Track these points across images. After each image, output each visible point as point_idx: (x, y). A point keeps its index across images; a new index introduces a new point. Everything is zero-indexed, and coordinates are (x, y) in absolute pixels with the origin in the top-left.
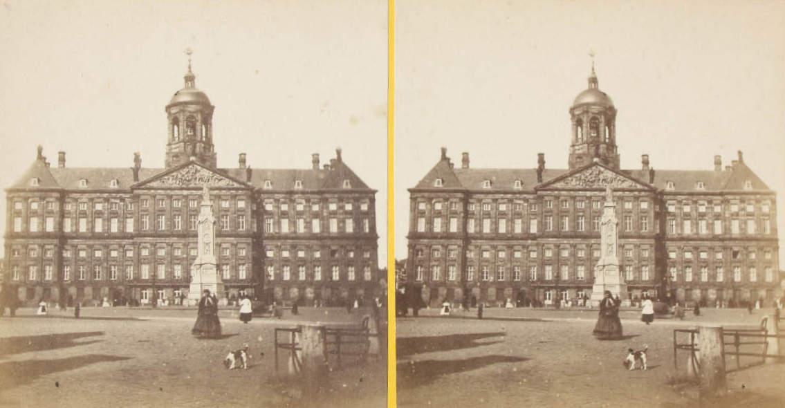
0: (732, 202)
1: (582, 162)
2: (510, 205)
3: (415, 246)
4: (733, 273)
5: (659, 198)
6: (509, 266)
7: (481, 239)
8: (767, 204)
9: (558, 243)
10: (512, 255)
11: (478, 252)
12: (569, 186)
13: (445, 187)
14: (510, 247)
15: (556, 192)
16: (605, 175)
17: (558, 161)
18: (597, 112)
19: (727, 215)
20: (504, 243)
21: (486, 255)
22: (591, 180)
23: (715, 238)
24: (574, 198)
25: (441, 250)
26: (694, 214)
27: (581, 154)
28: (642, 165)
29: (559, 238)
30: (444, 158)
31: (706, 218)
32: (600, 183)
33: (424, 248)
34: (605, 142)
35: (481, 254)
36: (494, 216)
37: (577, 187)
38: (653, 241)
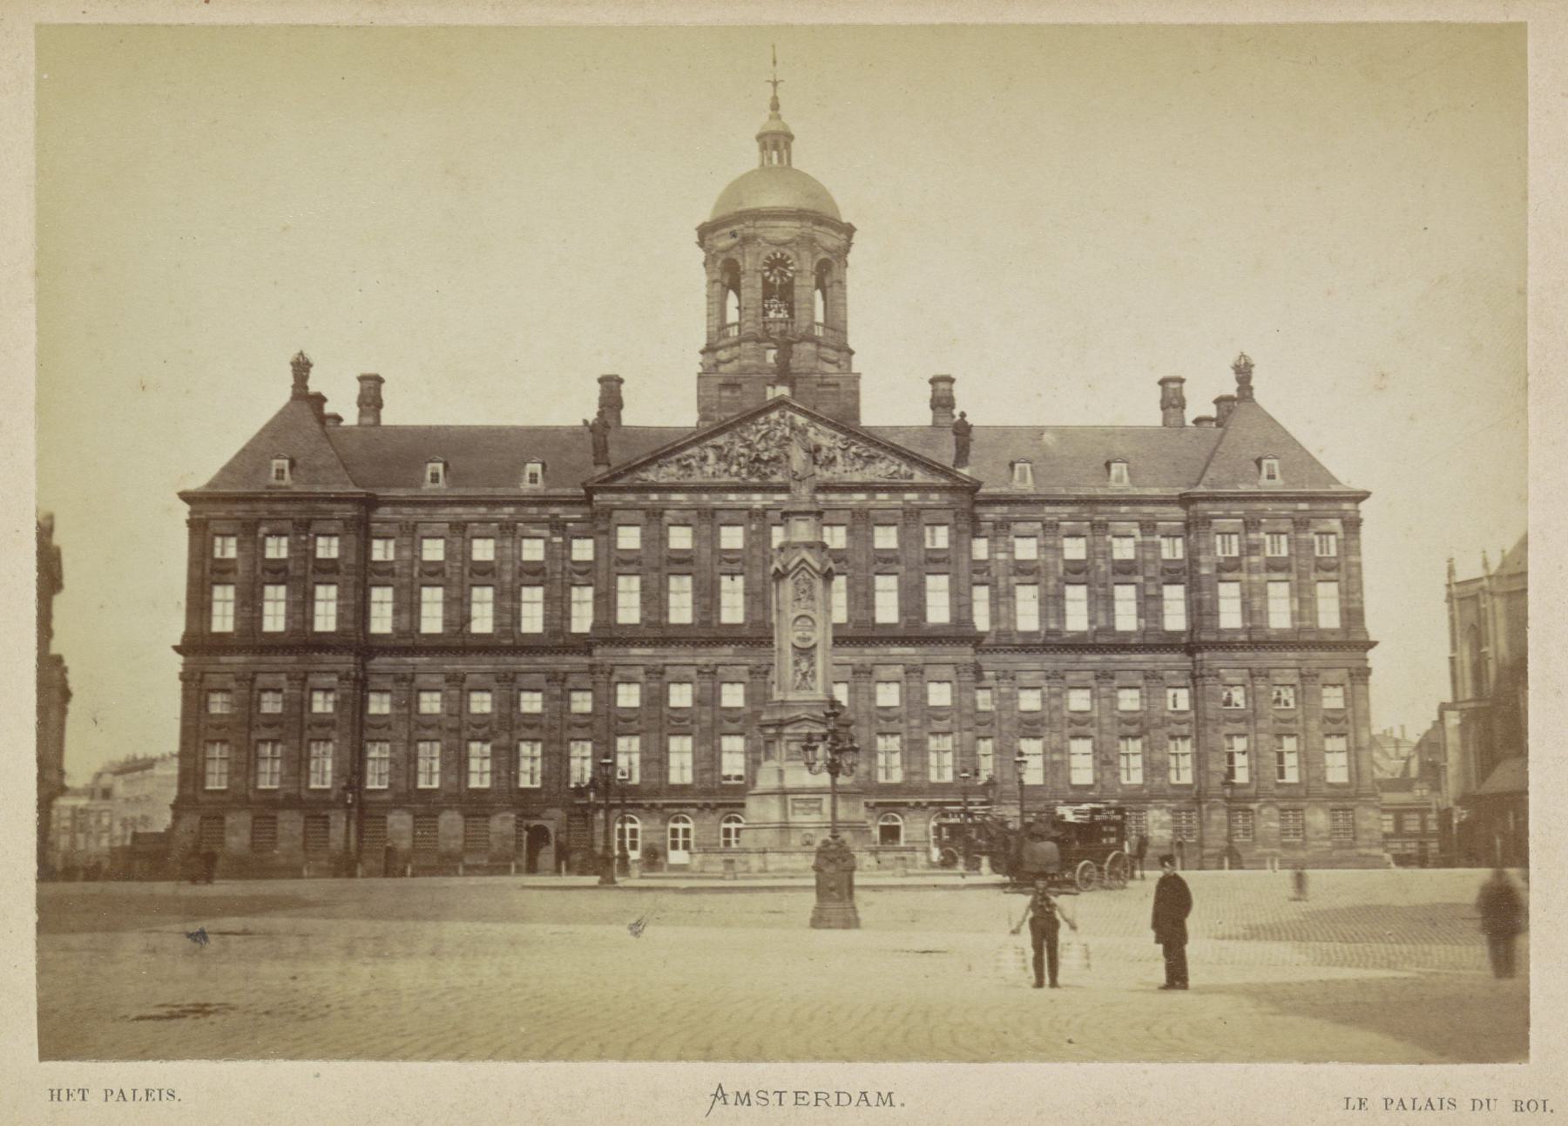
12: (697, 478)
15: (654, 497)
22: (765, 457)
31: (1139, 579)
36: (456, 579)
37: (725, 479)
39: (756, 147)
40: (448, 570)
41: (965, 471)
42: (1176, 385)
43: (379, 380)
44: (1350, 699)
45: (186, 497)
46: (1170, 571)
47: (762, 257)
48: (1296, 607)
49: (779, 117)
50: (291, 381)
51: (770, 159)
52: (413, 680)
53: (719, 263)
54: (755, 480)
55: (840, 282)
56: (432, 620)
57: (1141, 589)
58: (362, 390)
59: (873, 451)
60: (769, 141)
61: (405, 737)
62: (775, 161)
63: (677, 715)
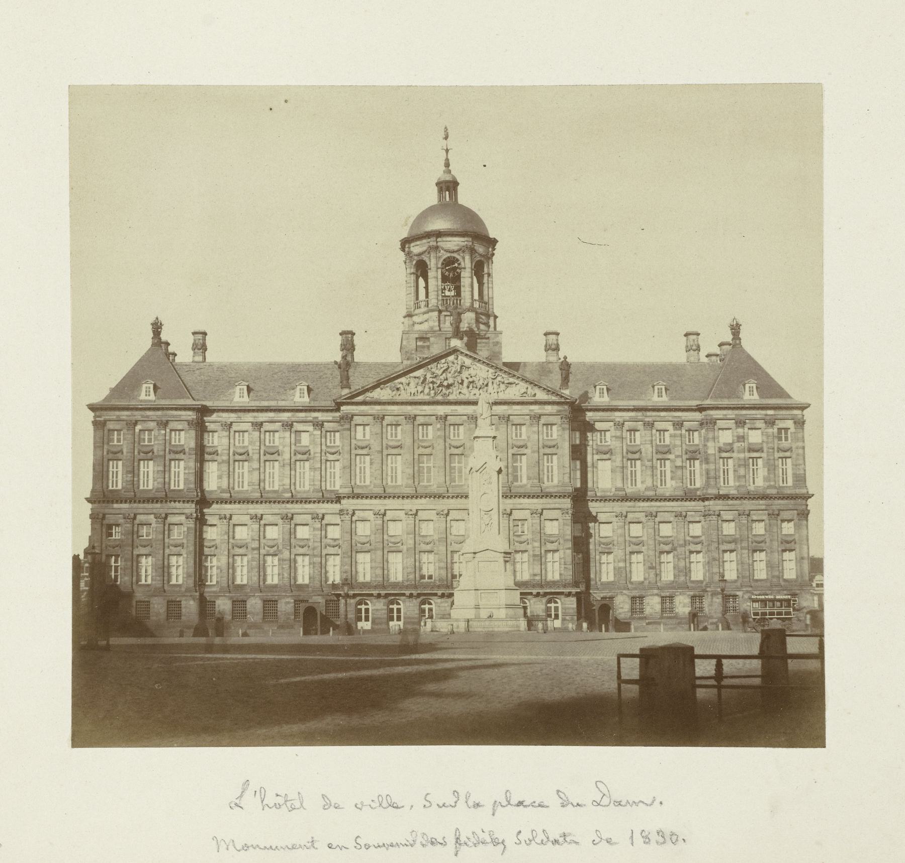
1: (428, 347)
2: (287, 434)
3: (104, 518)
5: (578, 416)
10: (292, 533)
11: (225, 528)
12: (404, 396)
15: (378, 407)
16: (472, 371)
17: (380, 348)
18: (456, 248)
19: (711, 451)
20: (277, 508)
22: (445, 383)
23: (689, 496)
26: (647, 450)
27: (426, 332)
31: (671, 457)
34: (471, 309)
35: (230, 534)
36: (256, 457)
37: (420, 397)
38: (567, 503)
39: (436, 189)
40: (251, 452)
41: (566, 392)
42: (694, 337)
43: (205, 334)
44: (798, 527)
45: (92, 408)
47: (442, 260)
48: (766, 474)
49: (450, 172)
50: (152, 335)
52: (230, 519)
53: (414, 262)
54: (439, 398)
55: (489, 275)
61: (226, 553)
63: (393, 540)
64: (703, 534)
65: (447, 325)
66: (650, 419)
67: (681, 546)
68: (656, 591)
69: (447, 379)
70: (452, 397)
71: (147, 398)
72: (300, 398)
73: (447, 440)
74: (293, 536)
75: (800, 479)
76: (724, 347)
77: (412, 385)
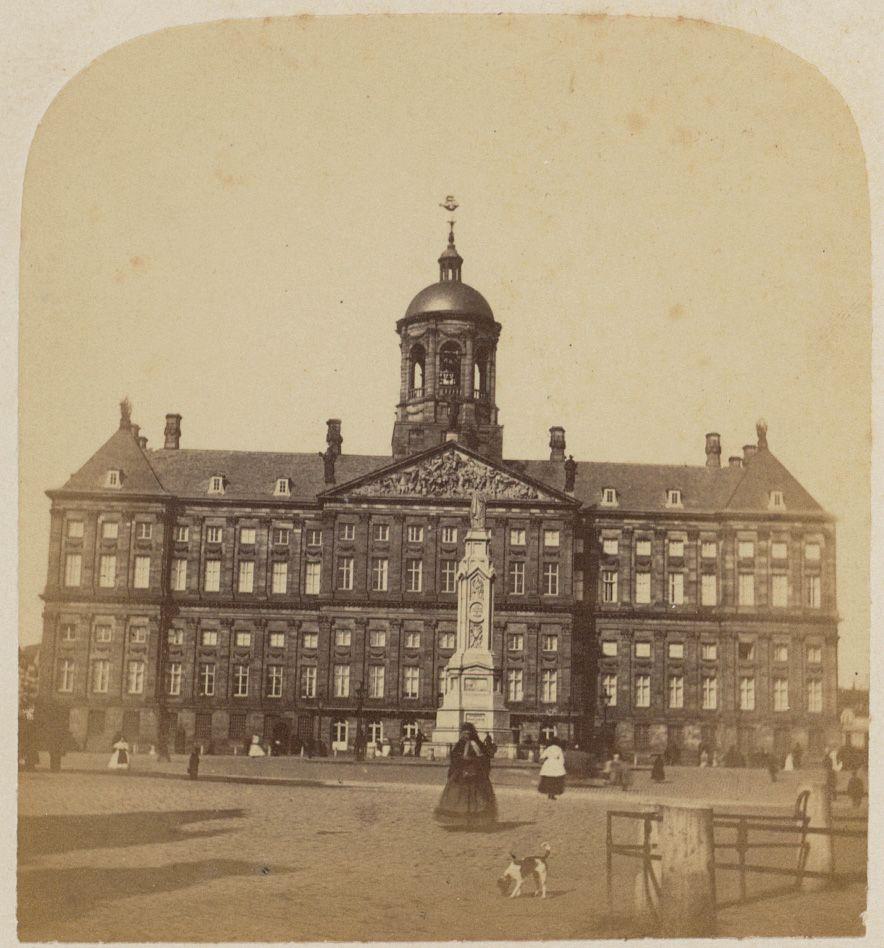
0: (742, 535)
1: (422, 440)
3: (59, 616)
4: (737, 690)
6: (258, 664)
7: (200, 606)
8: (817, 543)
9: (365, 616)
12: (394, 494)
13: (128, 488)
14: (261, 624)
15: (365, 506)
16: (468, 468)
17: (371, 437)
19: (729, 566)
21: (211, 639)
22: (439, 481)
23: (702, 614)
24: (401, 519)
25: (113, 627)
28: (550, 450)
29: (369, 606)
30: (126, 424)
31: (686, 570)
32: (460, 489)
33: (78, 621)
34: (471, 400)
35: (198, 638)
37: (412, 495)
38: (568, 618)
39: (438, 266)
40: (224, 549)
41: (571, 494)
42: (716, 438)
43: (178, 418)
45: (49, 494)
46: (706, 565)
48: (790, 592)
50: (120, 417)
51: (447, 276)
54: (431, 496)
56: (213, 583)
57: (686, 576)
58: (168, 424)
59: (511, 479)
60: (446, 263)
61: (192, 660)
62: (450, 277)
64: (718, 657)
65: (445, 417)
66: (663, 528)
67: (693, 670)
68: (662, 719)
69: (441, 476)
70: (445, 496)
71: (113, 486)
72: (280, 491)
73: (439, 544)
74: (266, 644)
75: (829, 600)
76: (749, 451)
77: (403, 481)
